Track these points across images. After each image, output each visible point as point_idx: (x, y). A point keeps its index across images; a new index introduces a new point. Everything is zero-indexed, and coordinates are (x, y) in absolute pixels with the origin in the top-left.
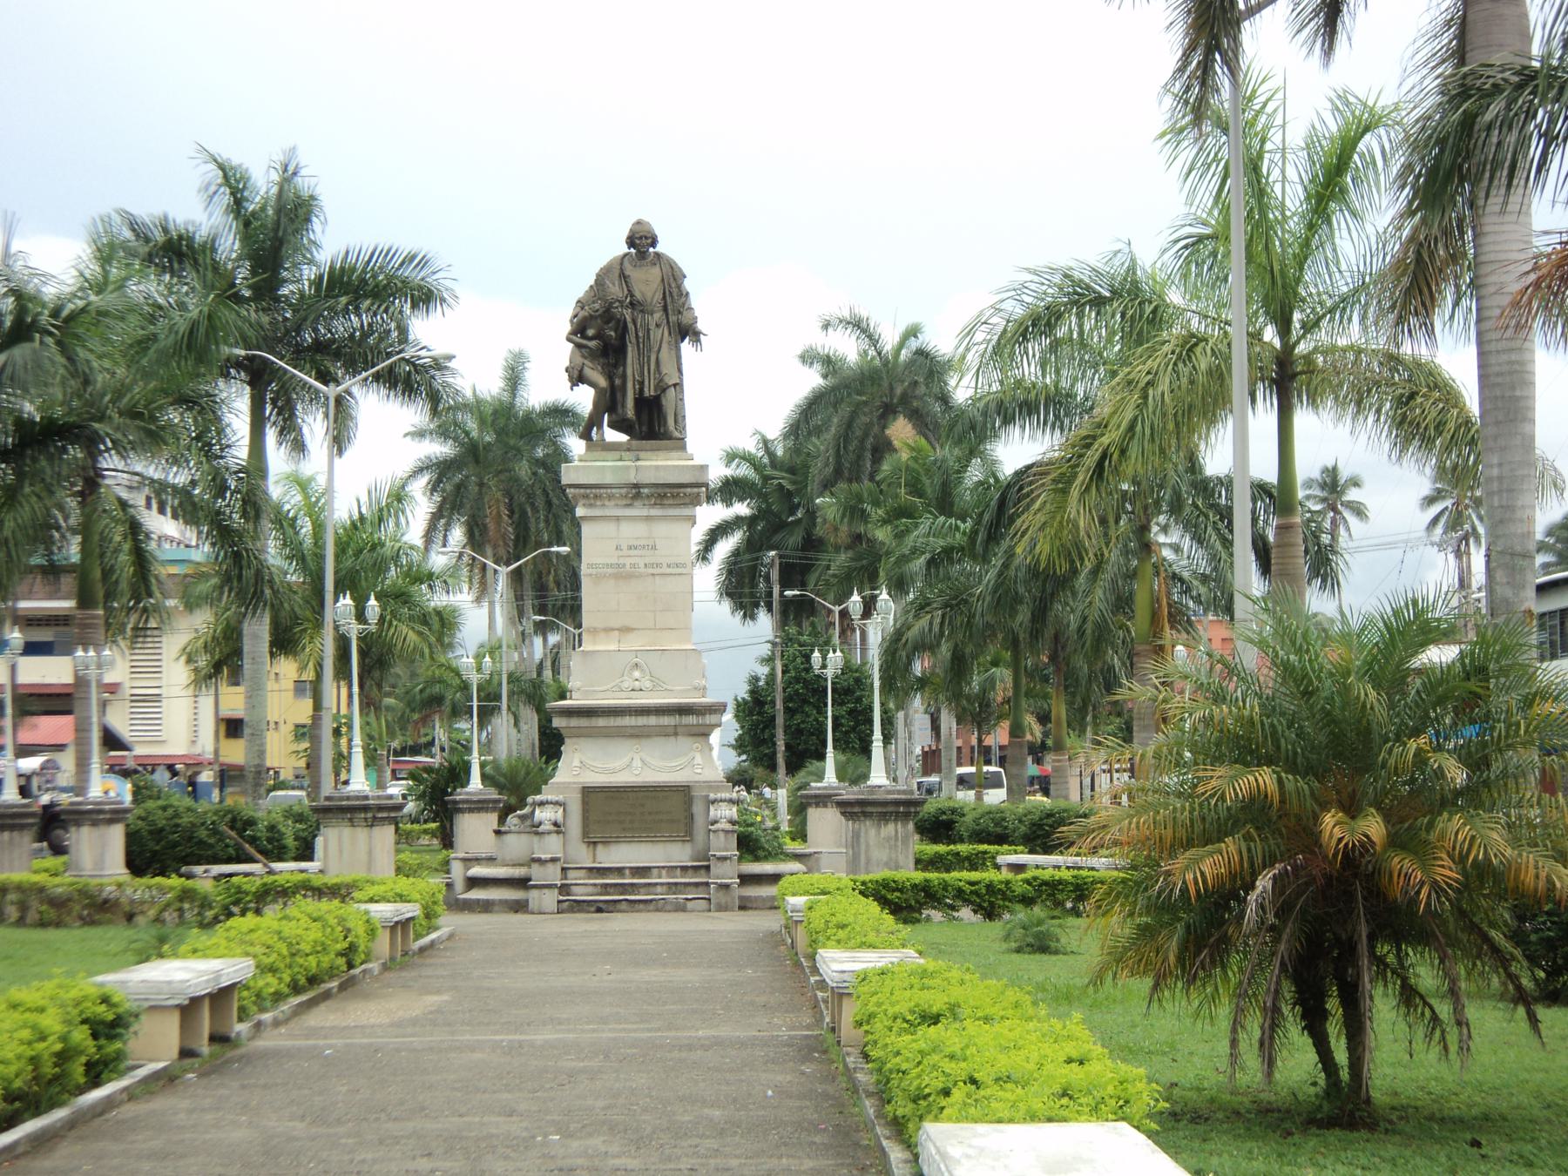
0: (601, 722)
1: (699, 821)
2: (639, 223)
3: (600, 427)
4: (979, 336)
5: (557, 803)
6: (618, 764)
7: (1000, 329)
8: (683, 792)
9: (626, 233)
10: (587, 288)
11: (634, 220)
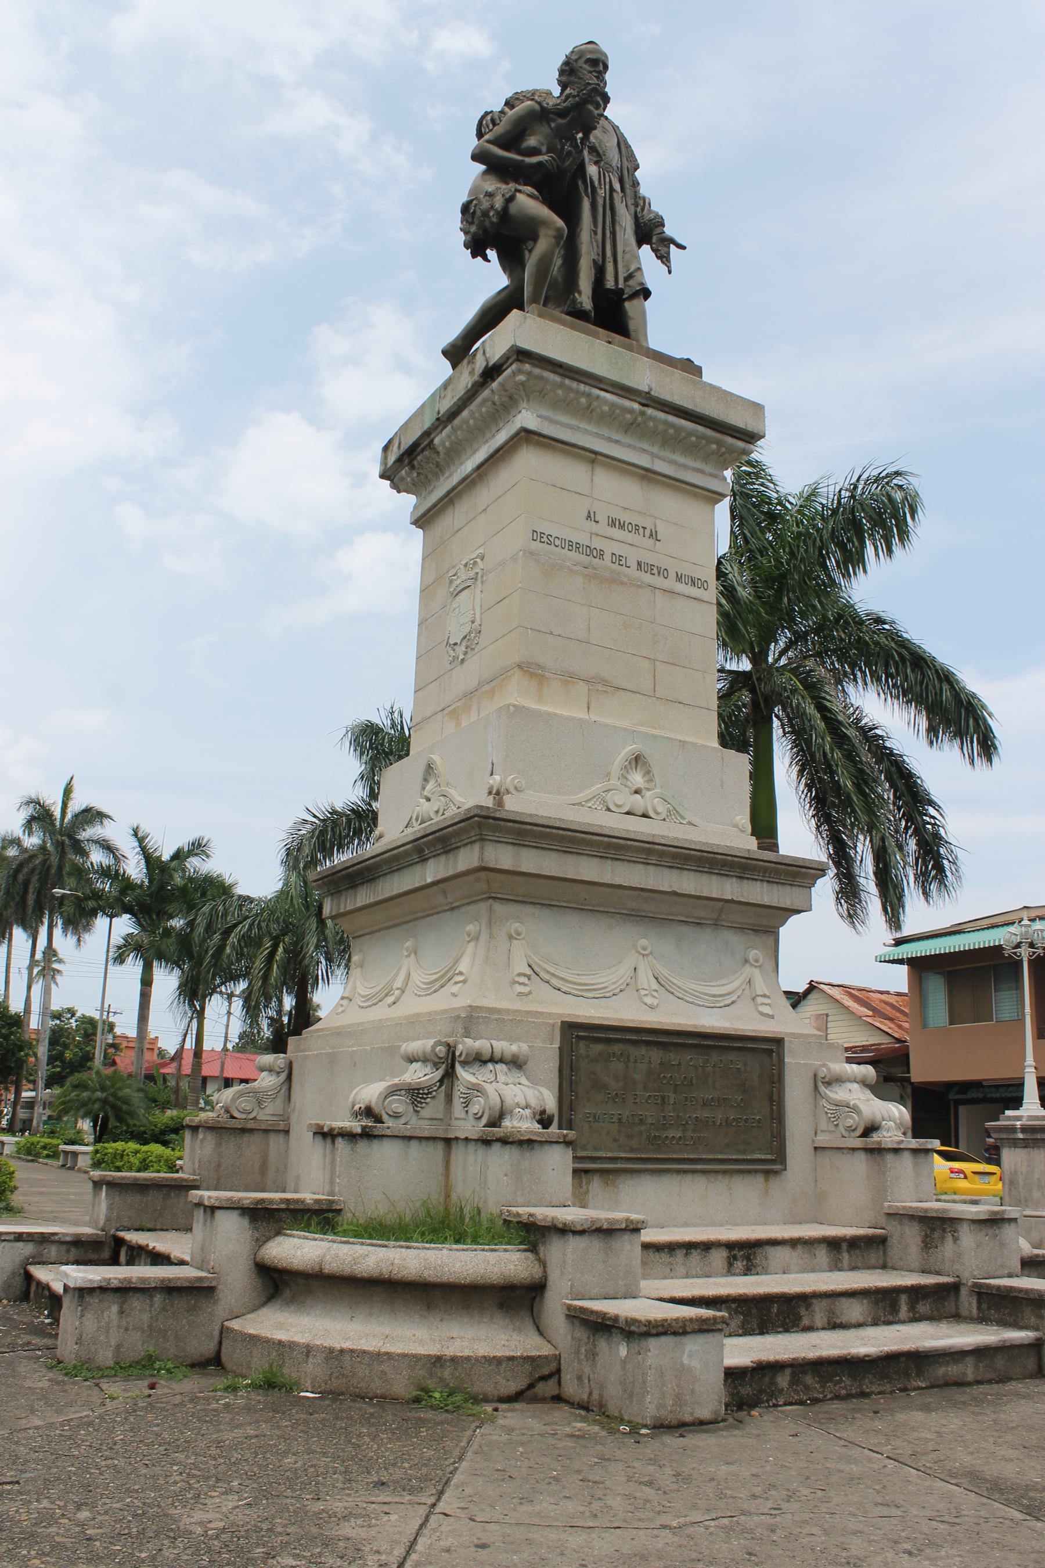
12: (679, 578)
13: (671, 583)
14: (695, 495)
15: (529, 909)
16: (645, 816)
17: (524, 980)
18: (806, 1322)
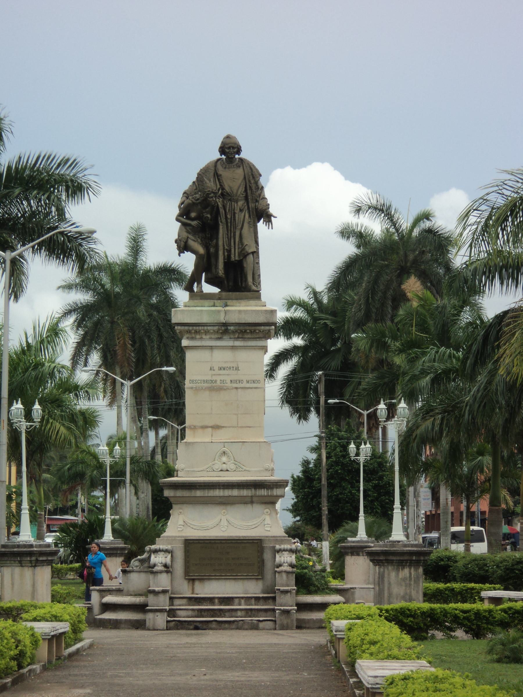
0: (199, 493)
1: (268, 565)
2: (228, 137)
3: (199, 283)
4: (472, 219)
5: (166, 551)
6: (210, 523)
7: (486, 214)
8: (257, 544)
9: (219, 145)
10: (191, 183)
11: (225, 135)
12: (248, 382)
13: (245, 385)
14: (255, 349)
15: (185, 505)
16: (227, 470)
17: (182, 527)
18: (223, 615)
